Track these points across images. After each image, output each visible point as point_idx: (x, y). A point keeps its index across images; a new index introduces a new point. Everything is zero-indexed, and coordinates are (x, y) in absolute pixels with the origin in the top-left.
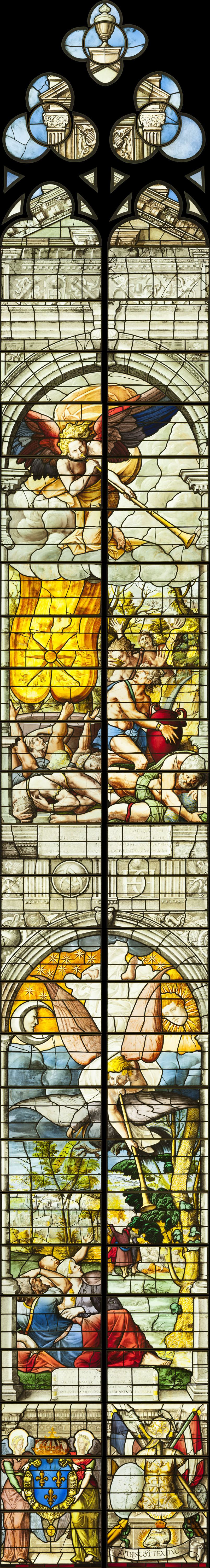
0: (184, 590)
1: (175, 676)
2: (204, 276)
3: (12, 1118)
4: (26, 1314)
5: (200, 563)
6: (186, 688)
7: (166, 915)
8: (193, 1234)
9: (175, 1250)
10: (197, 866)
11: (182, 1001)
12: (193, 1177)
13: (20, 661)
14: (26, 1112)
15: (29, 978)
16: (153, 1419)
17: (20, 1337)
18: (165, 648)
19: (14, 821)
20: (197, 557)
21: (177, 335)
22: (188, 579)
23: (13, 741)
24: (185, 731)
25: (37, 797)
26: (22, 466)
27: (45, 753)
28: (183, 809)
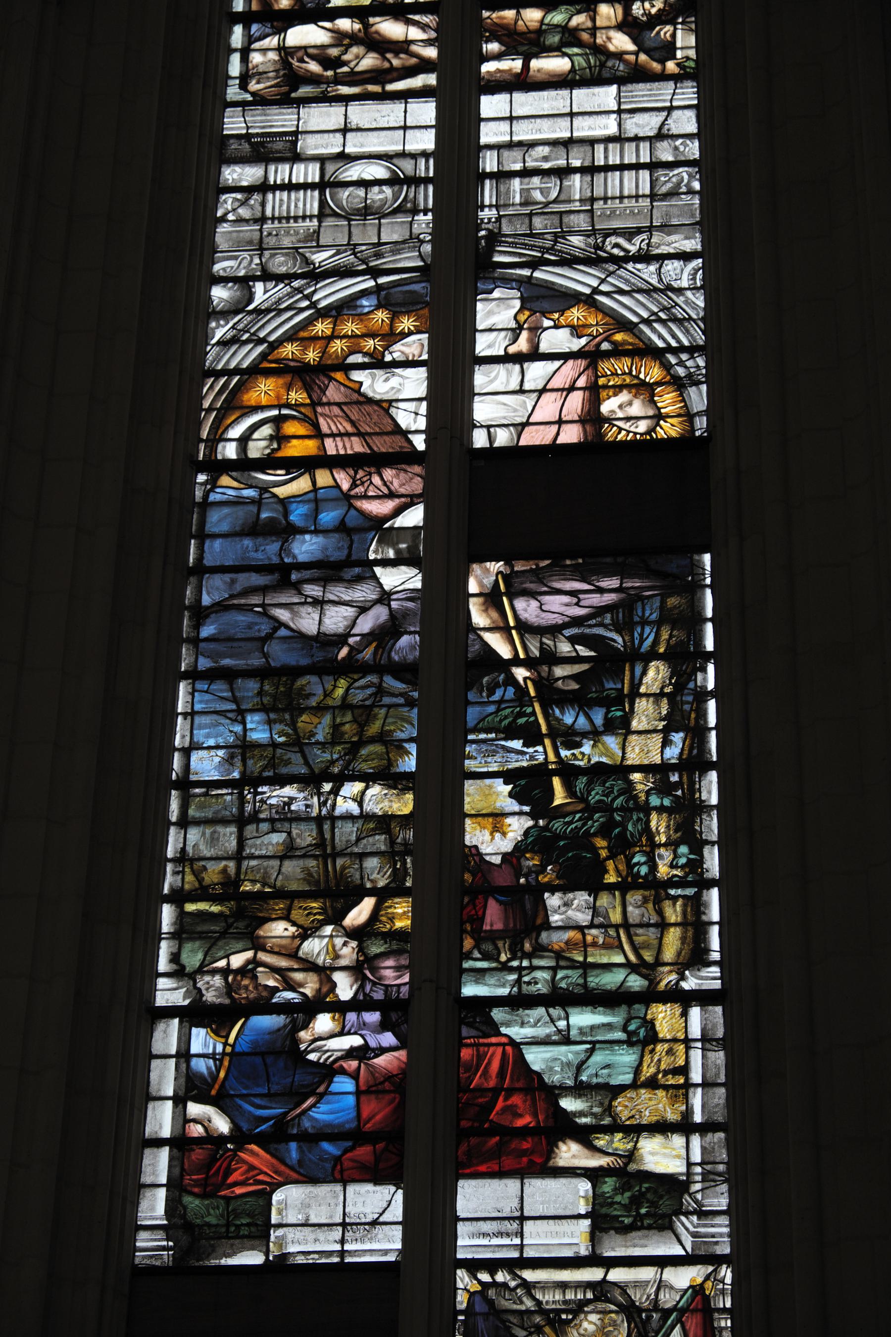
3: (206, 631)
4: (213, 1056)
7: (606, 236)
8: (683, 861)
9: (634, 897)
12: (677, 738)
14: (242, 618)
15: (266, 365)
16: (578, 1309)
17: (194, 1109)
25: (301, 60)
28: (643, 57)
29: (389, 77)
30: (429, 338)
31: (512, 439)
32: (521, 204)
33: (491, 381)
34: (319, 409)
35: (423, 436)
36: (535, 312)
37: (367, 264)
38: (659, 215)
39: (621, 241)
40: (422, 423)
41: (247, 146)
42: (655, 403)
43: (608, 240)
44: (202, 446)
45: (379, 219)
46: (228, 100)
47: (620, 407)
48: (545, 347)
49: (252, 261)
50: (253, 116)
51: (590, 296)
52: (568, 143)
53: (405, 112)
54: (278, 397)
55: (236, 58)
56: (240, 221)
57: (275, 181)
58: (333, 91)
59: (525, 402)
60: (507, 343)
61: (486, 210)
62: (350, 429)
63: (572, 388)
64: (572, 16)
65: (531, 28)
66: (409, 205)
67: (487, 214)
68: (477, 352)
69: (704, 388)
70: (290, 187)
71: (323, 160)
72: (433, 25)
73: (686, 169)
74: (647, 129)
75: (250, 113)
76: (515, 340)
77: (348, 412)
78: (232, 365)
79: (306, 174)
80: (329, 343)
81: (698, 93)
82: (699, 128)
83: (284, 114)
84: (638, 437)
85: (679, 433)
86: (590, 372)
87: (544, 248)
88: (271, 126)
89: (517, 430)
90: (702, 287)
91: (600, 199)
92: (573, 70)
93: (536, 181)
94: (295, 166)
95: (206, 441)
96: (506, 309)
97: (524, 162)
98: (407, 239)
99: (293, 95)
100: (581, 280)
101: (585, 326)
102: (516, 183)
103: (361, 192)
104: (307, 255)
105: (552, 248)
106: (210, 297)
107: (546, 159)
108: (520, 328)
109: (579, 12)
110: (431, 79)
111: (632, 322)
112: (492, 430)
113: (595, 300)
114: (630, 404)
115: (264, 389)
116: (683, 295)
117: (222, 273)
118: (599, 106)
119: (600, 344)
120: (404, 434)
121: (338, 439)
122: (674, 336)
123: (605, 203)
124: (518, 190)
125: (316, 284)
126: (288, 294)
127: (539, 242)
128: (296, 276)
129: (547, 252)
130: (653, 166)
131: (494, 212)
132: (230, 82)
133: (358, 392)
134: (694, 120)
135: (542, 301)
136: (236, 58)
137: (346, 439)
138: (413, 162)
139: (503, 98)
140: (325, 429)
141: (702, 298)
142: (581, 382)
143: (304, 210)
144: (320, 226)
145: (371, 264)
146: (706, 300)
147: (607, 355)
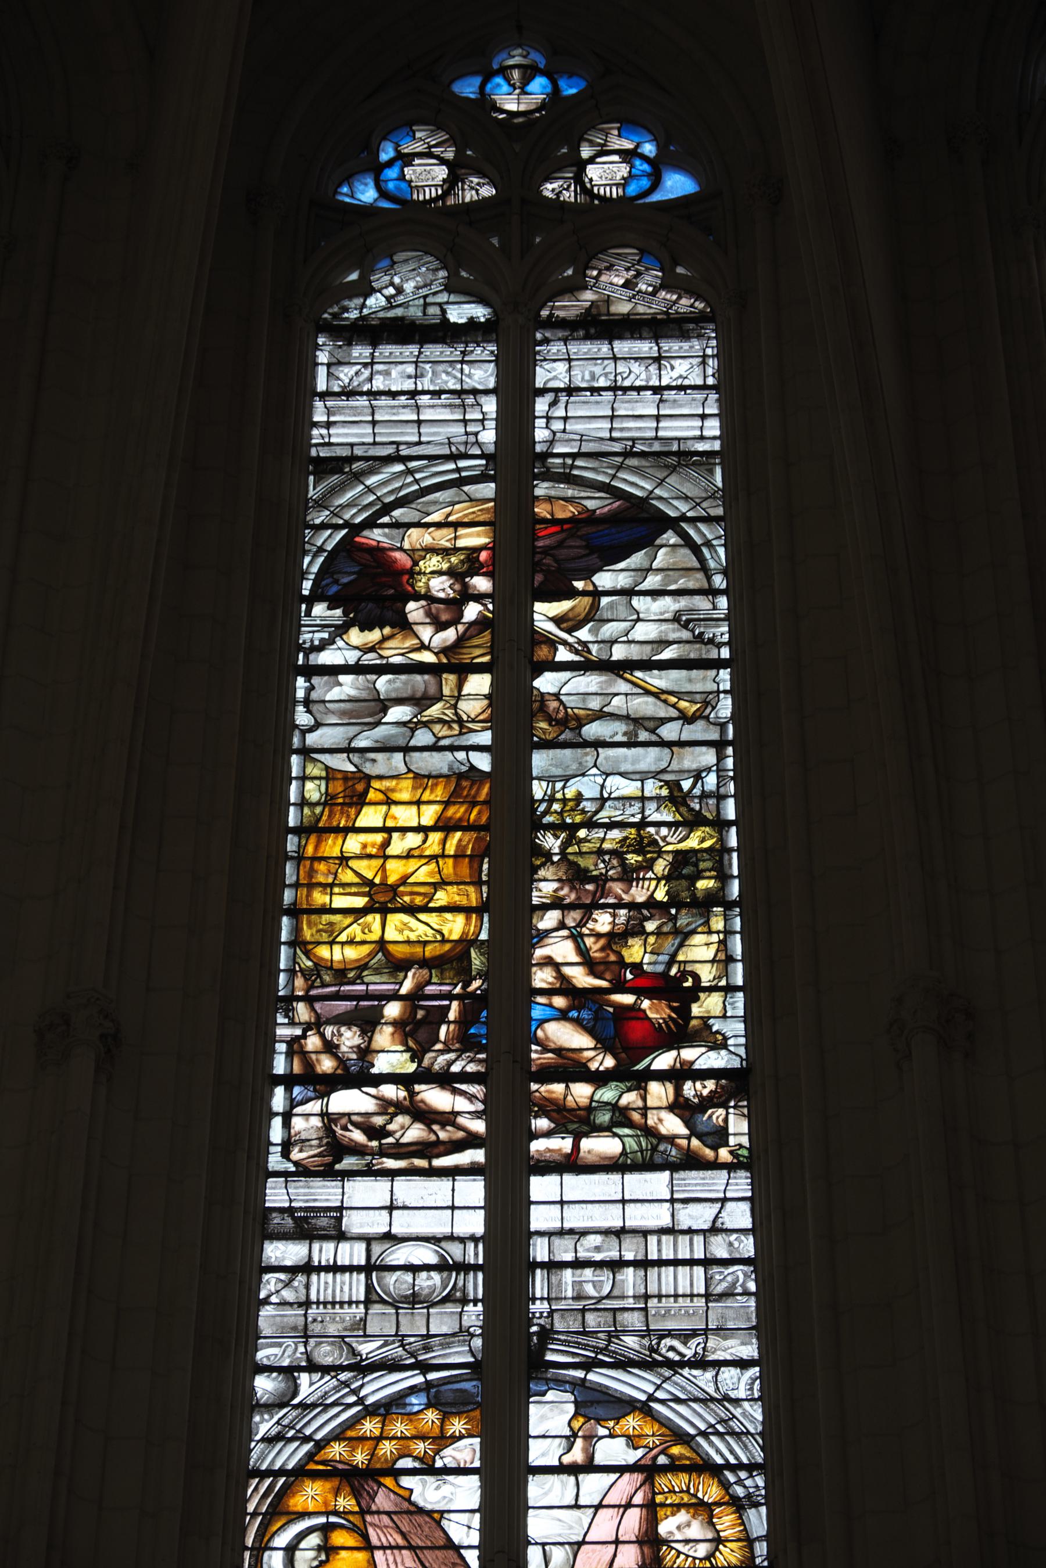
0: (686, 785)
1: (674, 919)
2: (710, 362)
5: (719, 746)
6: (698, 939)
7: (661, 1337)
10: (731, 1244)
11: (702, 1509)
13: (320, 898)
15: (312, 1466)
18: (650, 875)
19: (293, 1169)
20: (714, 735)
21: (661, 434)
22: (694, 766)
23: (298, 1032)
24: (696, 1010)
25: (345, 1128)
26: (338, 612)
27: (366, 1053)
28: (695, 1142)
29: (436, 1151)
30: (481, 1443)
31: (568, 1559)
32: (573, 1298)
33: (546, 1494)
34: (368, 1518)
35: (476, 1552)
36: (589, 1419)
37: (416, 1358)
38: (714, 1317)
39: (676, 1343)
40: (474, 1538)
41: (290, 1221)
42: (713, 1525)
43: (663, 1342)
44: (247, 1555)
45: (428, 1308)
46: (270, 1169)
47: (679, 1528)
48: (599, 1459)
49: (296, 1349)
50: (296, 1188)
51: (645, 1404)
52: (620, 1233)
53: (453, 1190)
54: (326, 1503)
55: (277, 1123)
56: (284, 1304)
57: (320, 1262)
58: (378, 1164)
59: (580, 1519)
60: (562, 1452)
61: (538, 1302)
62: (401, 1541)
63: (628, 1505)
64: (623, 1093)
65: (580, 1104)
66: (458, 1294)
67: (539, 1307)
68: (530, 1460)
69: (763, 1509)
70: (335, 1269)
71: (368, 1240)
72: (481, 1096)
73: (741, 1267)
74: (701, 1221)
75: (293, 1184)
76: (569, 1449)
77: (399, 1523)
78: (277, 1466)
79: (351, 1255)
80: (377, 1445)
81: (752, 1184)
82: (753, 1223)
83: (328, 1187)
84: (697, 1561)
85: (739, 1560)
86: (646, 1487)
87: (598, 1348)
88: (315, 1200)
89: (573, 1549)
90: (760, 1399)
91: (655, 1296)
92: (624, 1153)
93: (588, 1273)
94: (340, 1245)
95: (252, 1549)
96: (560, 1414)
97: (576, 1252)
98: (456, 1333)
99: (337, 1167)
100: (635, 1385)
101: (639, 1436)
102: (568, 1274)
103: (408, 1277)
104: (354, 1345)
105: (606, 1349)
106: (253, 1388)
107: (598, 1249)
108: (575, 1435)
109: (629, 1090)
110: (478, 1156)
111: (689, 1434)
112: (547, 1548)
113: (650, 1408)
114: (688, 1525)
115: (311, 1494)
116: (741, 1406)
117: (265, 1362)
118: (651, 1193)
119: (655, 1458)
120: (457, 1548)
121: (388, 1552)
122: (732, 1451)
123: (660, 1301)
124: (570, 1283)
125: (363, 1378)
126: (334, 1388)
127: (592, 1341)
128: (342, 1368)
129: (601, 1353)
130: (707, 1262)
131: (546, 1305)
132: (272, 1149)
133: (408, 1500)
134: (748, 1213)
135: (597, 1406)
136: (277, 1123)
137: (396, 1552)
138: (461, 1246)
139: (553, 1179)
140: (375, 1541)
141: (760, 1410)
142: (638, 1499)
143: (350, 1296)
144: (366, 1314)
145: (420, 1358)
146: (763, 1412)
147: (664, 1469)
